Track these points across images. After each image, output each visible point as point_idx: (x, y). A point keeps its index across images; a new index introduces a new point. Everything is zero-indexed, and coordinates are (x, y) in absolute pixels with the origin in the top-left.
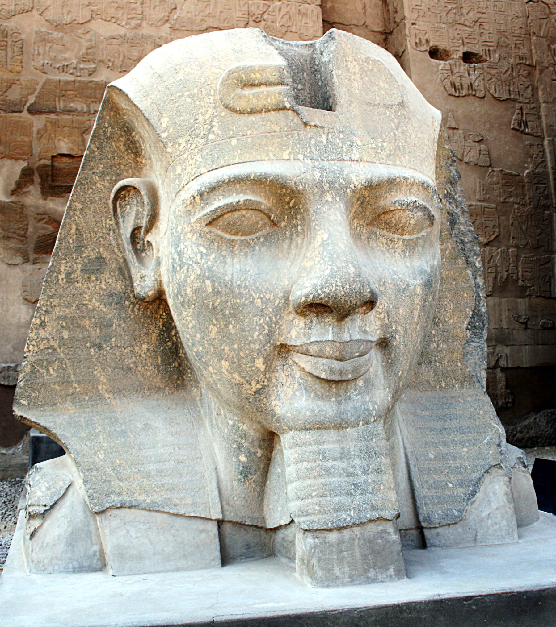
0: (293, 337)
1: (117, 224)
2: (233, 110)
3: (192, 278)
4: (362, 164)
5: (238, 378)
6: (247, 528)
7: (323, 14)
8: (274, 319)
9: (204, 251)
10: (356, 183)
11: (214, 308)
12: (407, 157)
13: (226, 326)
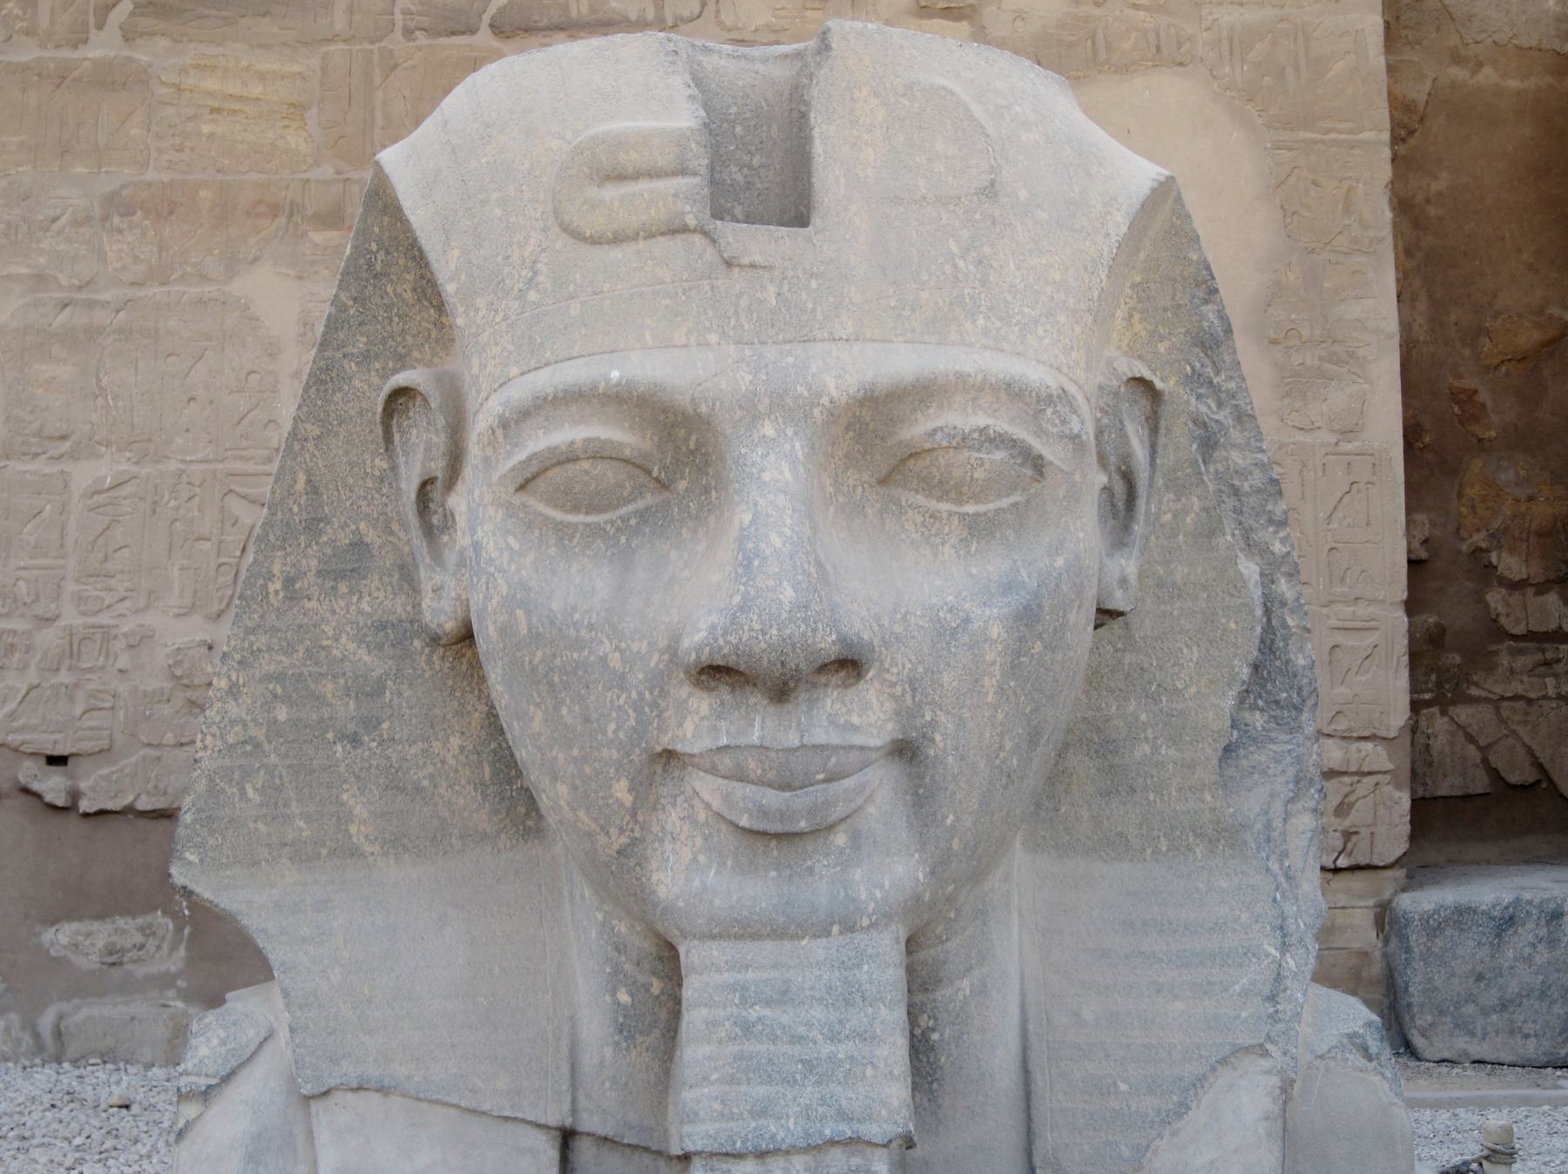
0: (689, 735)
1: (394, 468)
3: (494, 602)
4: (857, 348)
5: (586, 820)
6: (628, 1150)
8: (647, 695)
9: (516, 546)
10: (835, 394)
11: (533, 670)
12: (981, 322)
13: (556, 708)
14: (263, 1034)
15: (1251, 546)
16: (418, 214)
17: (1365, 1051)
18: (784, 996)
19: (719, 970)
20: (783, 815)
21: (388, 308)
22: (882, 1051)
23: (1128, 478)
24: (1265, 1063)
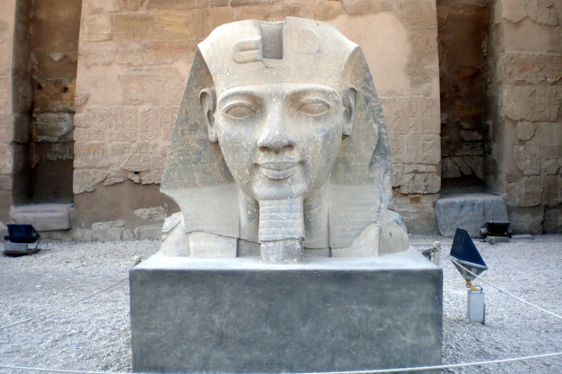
1: (203, 108)
15: (376, 122)
17: (398, 223)
18: (279, 211)
20: (278, 176)
21: (201, 76)
22: (298, 221)
23: (350, 108)
24: (376, 225)
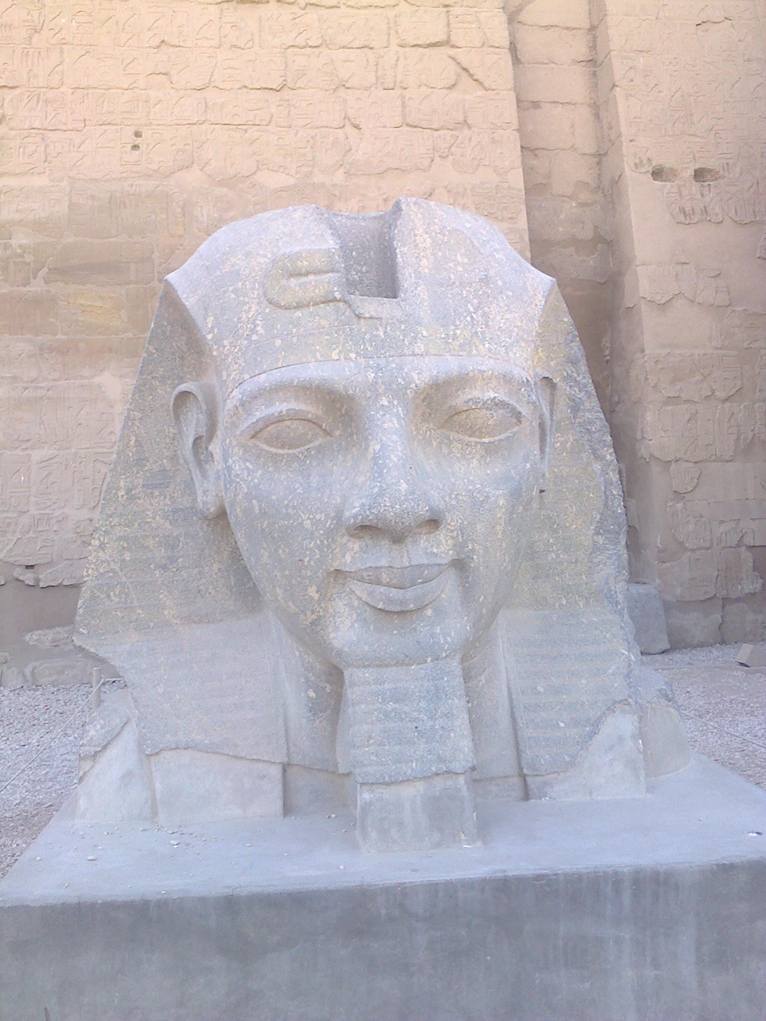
1: (180, 432)
2: (278, 305)
5: (293, 607)
7: (521, 139)
9: (251, 467)
10: (417, 382)
12: (487, 345)
13: (276, 550)
14: (124, 720)
16: (189, 301)
19: (369, 684)
22: (458, 722)
